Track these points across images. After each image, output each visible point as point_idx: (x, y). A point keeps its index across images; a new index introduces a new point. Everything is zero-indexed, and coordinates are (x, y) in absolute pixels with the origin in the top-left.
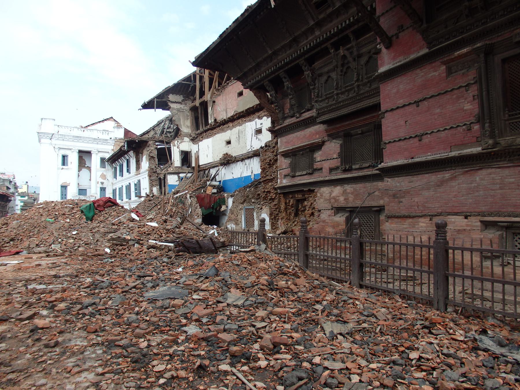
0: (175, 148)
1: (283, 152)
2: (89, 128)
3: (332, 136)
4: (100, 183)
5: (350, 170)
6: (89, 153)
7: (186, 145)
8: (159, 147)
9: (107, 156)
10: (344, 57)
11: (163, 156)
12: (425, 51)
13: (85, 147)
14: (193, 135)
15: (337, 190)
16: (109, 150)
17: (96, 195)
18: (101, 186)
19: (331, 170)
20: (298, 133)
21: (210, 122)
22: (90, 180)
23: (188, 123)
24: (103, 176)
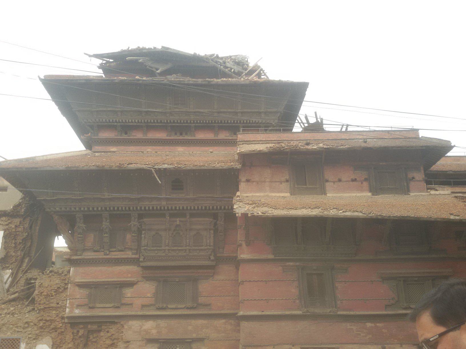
1: (79, 282)
3: (147, 279)
5: (162, 309)
10: (177, 226)
12: (271, 256)
15: (149, 325)
19: (143, 306)
20: (103, 268)
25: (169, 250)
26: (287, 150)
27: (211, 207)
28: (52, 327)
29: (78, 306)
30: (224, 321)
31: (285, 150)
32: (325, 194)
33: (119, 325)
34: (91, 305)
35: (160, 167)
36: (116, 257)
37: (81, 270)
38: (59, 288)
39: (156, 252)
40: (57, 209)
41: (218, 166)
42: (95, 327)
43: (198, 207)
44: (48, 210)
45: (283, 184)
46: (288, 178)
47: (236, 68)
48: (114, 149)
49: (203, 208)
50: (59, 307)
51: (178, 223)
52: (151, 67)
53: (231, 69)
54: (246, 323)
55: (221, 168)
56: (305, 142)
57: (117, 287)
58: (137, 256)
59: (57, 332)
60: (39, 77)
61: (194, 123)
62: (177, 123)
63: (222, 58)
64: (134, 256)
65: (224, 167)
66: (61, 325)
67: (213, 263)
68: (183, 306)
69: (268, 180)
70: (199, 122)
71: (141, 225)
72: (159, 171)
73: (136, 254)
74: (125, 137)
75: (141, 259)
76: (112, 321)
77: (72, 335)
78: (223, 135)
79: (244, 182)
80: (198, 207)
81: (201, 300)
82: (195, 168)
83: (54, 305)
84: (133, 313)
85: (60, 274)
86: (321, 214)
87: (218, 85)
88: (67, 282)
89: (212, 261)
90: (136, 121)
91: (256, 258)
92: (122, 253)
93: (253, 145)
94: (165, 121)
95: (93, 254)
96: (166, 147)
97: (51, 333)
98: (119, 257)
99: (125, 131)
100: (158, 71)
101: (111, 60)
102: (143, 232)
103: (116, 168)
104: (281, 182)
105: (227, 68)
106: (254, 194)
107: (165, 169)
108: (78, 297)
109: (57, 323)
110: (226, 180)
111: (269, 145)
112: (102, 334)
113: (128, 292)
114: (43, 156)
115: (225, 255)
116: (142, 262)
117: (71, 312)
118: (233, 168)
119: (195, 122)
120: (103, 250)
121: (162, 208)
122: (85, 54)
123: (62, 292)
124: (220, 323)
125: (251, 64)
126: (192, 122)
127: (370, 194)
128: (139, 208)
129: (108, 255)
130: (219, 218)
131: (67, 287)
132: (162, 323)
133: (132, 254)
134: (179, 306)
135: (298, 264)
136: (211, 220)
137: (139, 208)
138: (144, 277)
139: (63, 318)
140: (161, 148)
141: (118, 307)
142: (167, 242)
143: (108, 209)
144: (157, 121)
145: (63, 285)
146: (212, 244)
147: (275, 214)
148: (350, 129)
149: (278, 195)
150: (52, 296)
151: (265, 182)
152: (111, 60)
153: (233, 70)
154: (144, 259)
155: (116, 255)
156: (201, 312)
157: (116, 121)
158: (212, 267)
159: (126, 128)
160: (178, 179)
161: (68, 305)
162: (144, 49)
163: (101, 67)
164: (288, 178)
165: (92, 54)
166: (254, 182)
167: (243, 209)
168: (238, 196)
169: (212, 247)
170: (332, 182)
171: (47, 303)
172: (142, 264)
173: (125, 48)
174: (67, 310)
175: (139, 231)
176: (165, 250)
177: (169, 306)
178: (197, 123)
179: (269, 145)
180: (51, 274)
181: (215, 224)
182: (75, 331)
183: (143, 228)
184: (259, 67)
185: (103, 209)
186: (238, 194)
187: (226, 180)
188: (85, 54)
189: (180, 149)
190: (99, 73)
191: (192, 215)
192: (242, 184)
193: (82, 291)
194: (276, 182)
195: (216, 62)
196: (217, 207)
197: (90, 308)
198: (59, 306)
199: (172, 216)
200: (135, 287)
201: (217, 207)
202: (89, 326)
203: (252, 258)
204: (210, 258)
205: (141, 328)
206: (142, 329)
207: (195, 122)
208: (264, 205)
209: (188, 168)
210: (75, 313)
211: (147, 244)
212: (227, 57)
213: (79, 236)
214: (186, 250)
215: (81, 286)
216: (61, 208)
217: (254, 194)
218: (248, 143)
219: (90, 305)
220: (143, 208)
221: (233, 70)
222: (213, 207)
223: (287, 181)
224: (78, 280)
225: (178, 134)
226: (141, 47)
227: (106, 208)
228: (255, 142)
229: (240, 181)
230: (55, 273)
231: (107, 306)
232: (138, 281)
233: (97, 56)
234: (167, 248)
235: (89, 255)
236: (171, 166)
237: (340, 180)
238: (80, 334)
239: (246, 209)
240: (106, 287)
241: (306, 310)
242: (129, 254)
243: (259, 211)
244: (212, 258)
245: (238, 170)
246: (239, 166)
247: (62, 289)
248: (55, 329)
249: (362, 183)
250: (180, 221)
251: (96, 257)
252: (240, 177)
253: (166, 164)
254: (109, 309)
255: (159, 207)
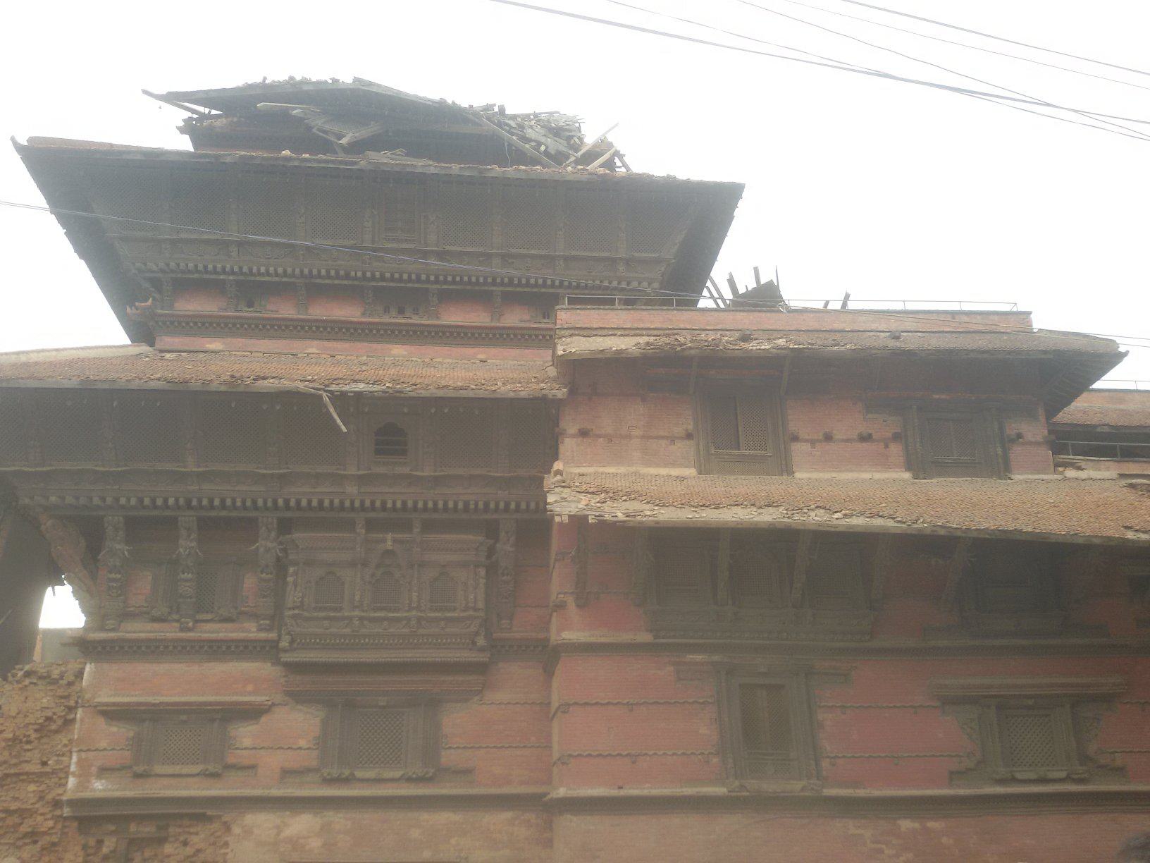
1: (107, 704)
3: (298, 697)
10: (388, 553)
15: (301, 824)
19: (286, 773)
25: (361, 619)
26: (693, 352)
27: (481, 505)
28: (25, 828)
29: (104, 771)
30: (509, 815)
31: (687, 353)
32: (791, 473)
33: (216, 825)
34: (140, 769)
35: (346, 388)
36: (213, 636)
37: (115, 670)
38: (48, 719)
39: (326, 623)
40: (53, 499)
41: (504, 390)
42: (148, 829)
43: (446, 503)
44: (27, 501)
45: (679, 444)
46: (690, 427)
47: (552, 144)
48: (215, 345)
49: (461, 505)
50: (47, 773)
51: (389, 545)
52: (326, 132)
53: (539, 144)
54: (575, 819)
55: (512, 395)
56: (737, 334)
57: (213, 720)
58: (273, 635)
59: (38, 846)
60: (13, 139)
61: (437, 282)
62: (392, 279)
63: (514, 117)
64: (263, 635)
65: (523, 394)
66: (50, 823)
67: (483, 657)
68: (398, 774)
69: (637, 432)
70: (450, 278)
71: (285, 550)
72: (341, 399)
73: (269, 630)
74: (247, 313)
75: (284, 644)
76: (197, 813)
77: (81, 853)
78: (514, 318)
79: (573, 436)
80: (446, 503)
81: (448, 758)
82: (440, 393)
83: (34, 768)
84: (257, 792)
85: (55, 682)
86: (786, 520)
87: (506, 182)
88: (72, 703)
89: (482, 650)
90: (280, 270)
91: (603, 640)
92: (229, 625)
93: (599, 339)
94: (359, 274)
95: (149, 626)
96: (359, 345)
97: (19, 848)
98: (221, 635)
99: (249, 297)
100: (344, 141)
101: (214, 112)
102: (291, 570)
103: (223, 388)
104: (673, 440)
105: (528, 140)
106: (601, 470)
107: (359, 395)
108: (103, 744)
109: (40, 818)
110: (528, 430)
111: (643, 340)
112: (168, 848)
113: (245, 734)
114: (18, 353)
115: (518, 635)
116: (286, 651)
117: (82, 786)
118: (544, 398)
119: (441, 278)
120: (175, 617)
121: (347, 504)
122: (145, 92)
123: (56, 732)
124: (497, 820)
125: (590, 139)
126: (432, 278)
127: (907, 475)
128: (280, 502)
129: (190, 630)
130: (502, 535)
131: (72, 716)
132: (340, 820)
133: (260, 630)
134: (388, 774)
135: (716, 658)
136: (481, 538)
137: (280, 502)
138: (290, 694)
139: (57, 804)
140: (346, 345)
141: (215, 775)
142: (357, 598)
143: (194, 503)
144: (337, 272)
145: (60, 711)
146: (481, 605)
147: (661, 518)
148: (851, 306)
149: (663, 471)
150: (29, 742)
151: (629, 437)
152: (214, 112)
153: (543, 148)
154: (292, 642)
155: (213, 631)
156: (444, 792)
157: (224, 268)
158: (481, 669)
159: (251, 290)
160: (393, 424)
161: (73, 768)
162: (305, 82)
163: (189, 128)
164: (690, 427)
165: (163, 91)
166: (599, 436)
167: (573, 505)
168: (559, 472)
169: (482, 614)
170: (806, 441)
171: (14, 761)
172: (286, 657)
173: (254, 78)
174: (72, 782)
175: (281, 567)
176: (350, 618)
177: (359, 774)
178: (445, 282)
179: (643, 340)
180: (27, 682)
181: (491, 552)
182: (92, 842)
183: (291, 557)
184: (610, 145)
185: (181, 501)
186: (558, 465)
187: (528, 430)
188: (145, 92)
189: (398, 350)
190: (184, 144)
191: (428, 526)
192: (567, 440)
193: (115, 729)
194: (657, 438)
195: (500, 125)
196: (497, 505)
197: (138, 776)
198: (48, 769)
199: (371, 525)
200: (263, 719)
201: (497, 505)
202: (133, 828)
203: (593, 640)
204: (474, 643)
205: (278, 834)
206: (283, 835)
207: (441, 278)
208: (629, 495)
209: (424, 393)
210: (95, 790)
211: (302, 602)
212: (528, 115)
213: (113, 576)
214: (409, 619)
215: (113, 714)
216: (63, 498)
217: (601, 470)
218: (585, 333)
219: (135, 768)
220: (292, 503)
221: (543, 148)
222: (486, 505)
223: (689, 436)
224: (106, 697)
225: (394, 312)
226: (298, 78)
227: (188, 502)
228: (605, 332)
229: (563, 433)
230: (41, 678)
231: (185, 770)
232: (273, 705)
233: (175, 98)
234: (357, 613)
235: (138, 630)
236: (376, 388)
237: (828, 438)
238: (105, 850)
239: (580, 506)
240: (184, 717)
241: (737, 783)
242: (250, 631)
243: (617, 511)
244: (481, 641)
245: (558, 403)
246: (561, 393)
247: (60, 722)
248: (33, 836)
249: (886, 446)
250: (395, 541)
251: (160, 635)
252: (563, 424)
253: (361, 381)
254: (190, 780)
255: (336, 501)
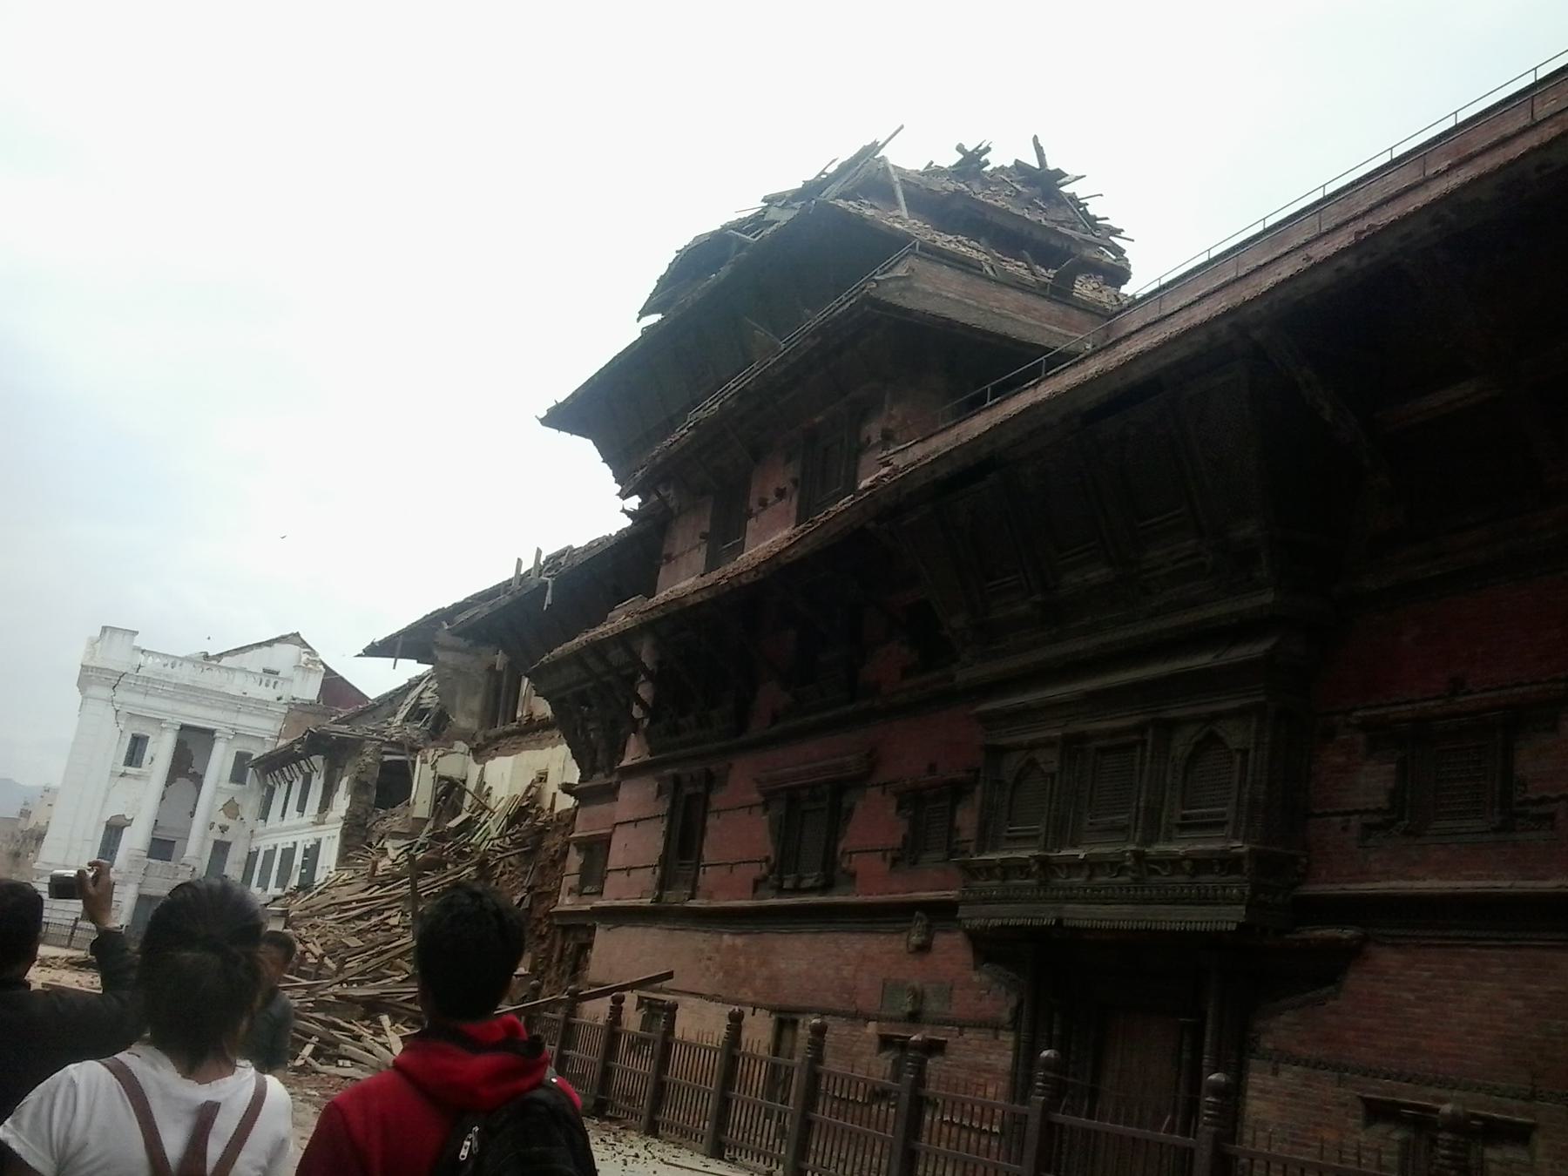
0: (427, 767)
2: (225, 661)
4: (216, 828)
6: (208, 735)
7: (456, 763)
8: (387, 758)
9: (257, 752)
11: (390, 786)
13: (199, 716)
14: (480, 740)
16: (266, 732)
17: (195, 863)
18: (218, 837)
21: (519, 715)
22: (192, 814)
23: (476, 704)
24: (231, 809)
